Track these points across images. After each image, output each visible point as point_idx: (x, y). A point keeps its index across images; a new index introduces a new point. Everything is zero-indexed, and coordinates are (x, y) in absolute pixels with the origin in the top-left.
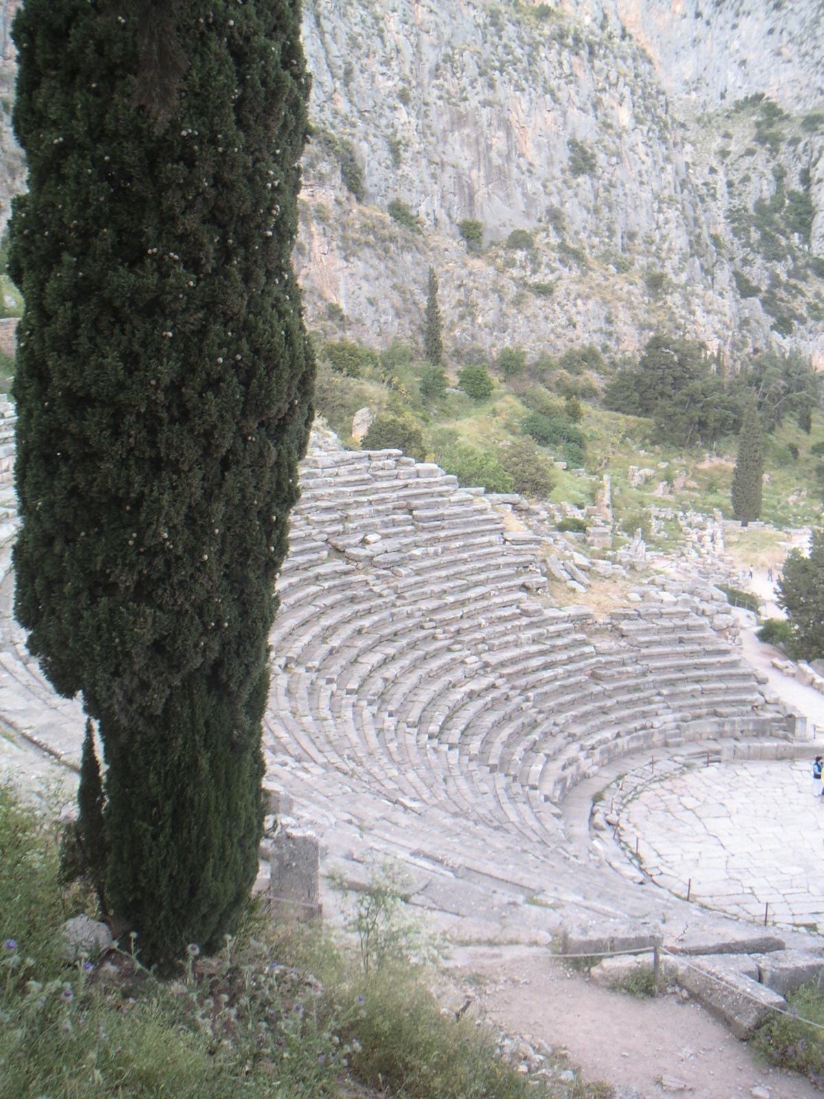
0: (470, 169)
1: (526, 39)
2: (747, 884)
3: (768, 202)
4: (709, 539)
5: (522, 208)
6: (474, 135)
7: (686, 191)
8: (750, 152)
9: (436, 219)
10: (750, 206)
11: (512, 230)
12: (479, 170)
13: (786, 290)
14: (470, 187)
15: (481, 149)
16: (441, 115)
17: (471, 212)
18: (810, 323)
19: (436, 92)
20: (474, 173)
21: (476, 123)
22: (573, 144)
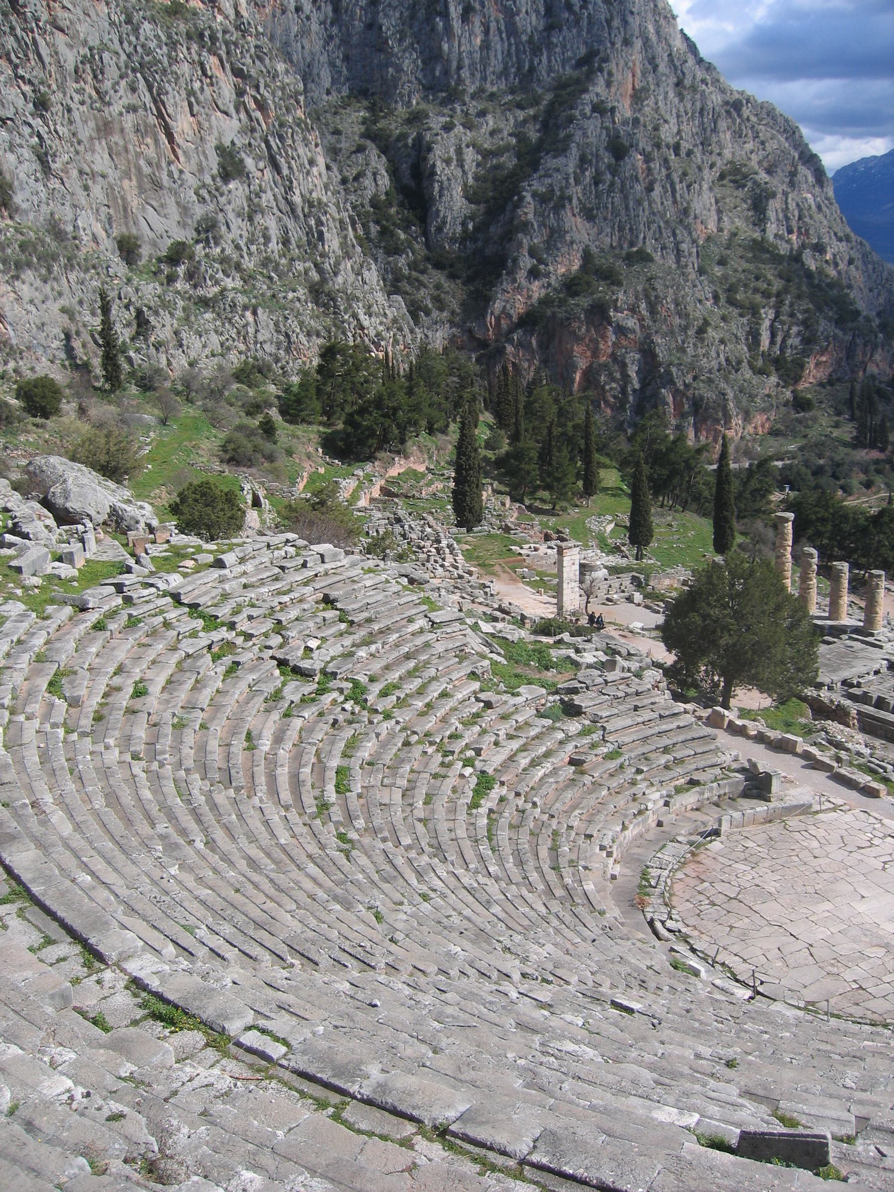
0: (121, 179)
1: (164, 38)
2: (848, 975)
3: (383, 197)
4: (447, 551)
5: (177, 217)
6: (121, 143)
7: (329, 193)
8: (360, 149)
9: (93, 235)
10: (366, 201)
11: (169, 242)
12: (130, 179)
13: (410, 284)
14: (124, 199)
15: (130, 157)
16: (86, 122)
17: (126, 224)
18: (435, 314)
19: (77, 97)
20: (126, 183)
21: (122, 130)
22: (220, 149)
